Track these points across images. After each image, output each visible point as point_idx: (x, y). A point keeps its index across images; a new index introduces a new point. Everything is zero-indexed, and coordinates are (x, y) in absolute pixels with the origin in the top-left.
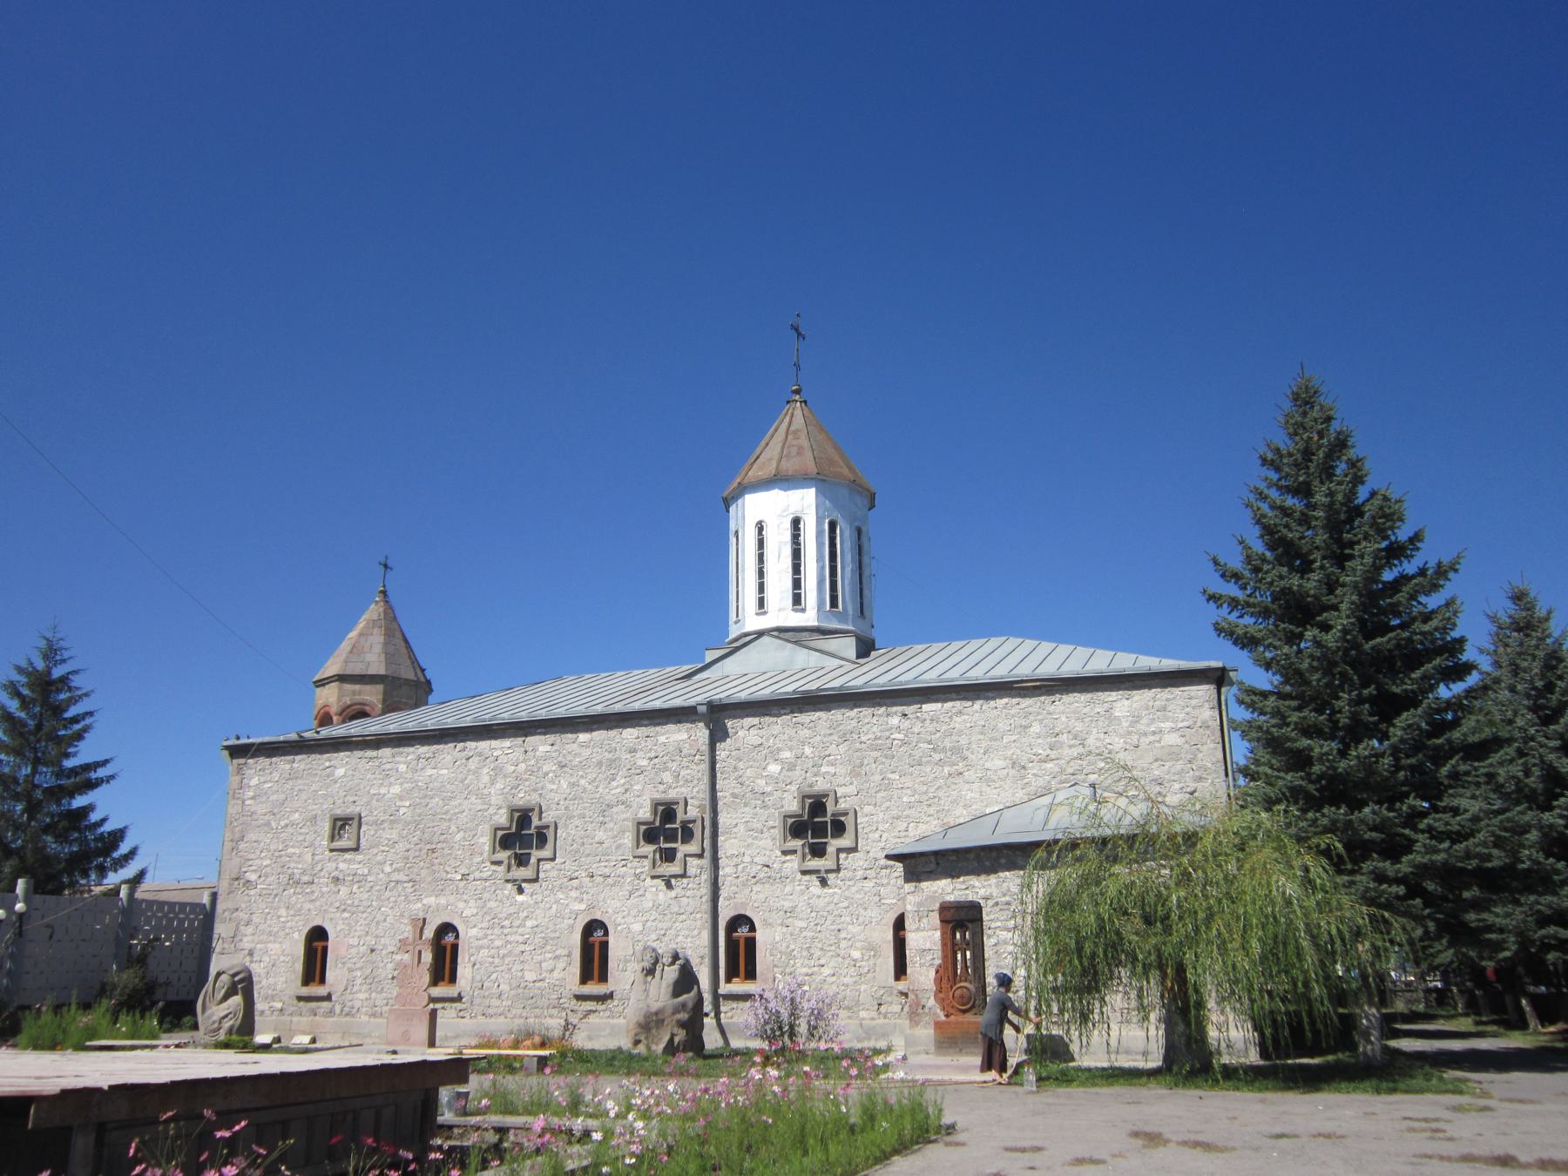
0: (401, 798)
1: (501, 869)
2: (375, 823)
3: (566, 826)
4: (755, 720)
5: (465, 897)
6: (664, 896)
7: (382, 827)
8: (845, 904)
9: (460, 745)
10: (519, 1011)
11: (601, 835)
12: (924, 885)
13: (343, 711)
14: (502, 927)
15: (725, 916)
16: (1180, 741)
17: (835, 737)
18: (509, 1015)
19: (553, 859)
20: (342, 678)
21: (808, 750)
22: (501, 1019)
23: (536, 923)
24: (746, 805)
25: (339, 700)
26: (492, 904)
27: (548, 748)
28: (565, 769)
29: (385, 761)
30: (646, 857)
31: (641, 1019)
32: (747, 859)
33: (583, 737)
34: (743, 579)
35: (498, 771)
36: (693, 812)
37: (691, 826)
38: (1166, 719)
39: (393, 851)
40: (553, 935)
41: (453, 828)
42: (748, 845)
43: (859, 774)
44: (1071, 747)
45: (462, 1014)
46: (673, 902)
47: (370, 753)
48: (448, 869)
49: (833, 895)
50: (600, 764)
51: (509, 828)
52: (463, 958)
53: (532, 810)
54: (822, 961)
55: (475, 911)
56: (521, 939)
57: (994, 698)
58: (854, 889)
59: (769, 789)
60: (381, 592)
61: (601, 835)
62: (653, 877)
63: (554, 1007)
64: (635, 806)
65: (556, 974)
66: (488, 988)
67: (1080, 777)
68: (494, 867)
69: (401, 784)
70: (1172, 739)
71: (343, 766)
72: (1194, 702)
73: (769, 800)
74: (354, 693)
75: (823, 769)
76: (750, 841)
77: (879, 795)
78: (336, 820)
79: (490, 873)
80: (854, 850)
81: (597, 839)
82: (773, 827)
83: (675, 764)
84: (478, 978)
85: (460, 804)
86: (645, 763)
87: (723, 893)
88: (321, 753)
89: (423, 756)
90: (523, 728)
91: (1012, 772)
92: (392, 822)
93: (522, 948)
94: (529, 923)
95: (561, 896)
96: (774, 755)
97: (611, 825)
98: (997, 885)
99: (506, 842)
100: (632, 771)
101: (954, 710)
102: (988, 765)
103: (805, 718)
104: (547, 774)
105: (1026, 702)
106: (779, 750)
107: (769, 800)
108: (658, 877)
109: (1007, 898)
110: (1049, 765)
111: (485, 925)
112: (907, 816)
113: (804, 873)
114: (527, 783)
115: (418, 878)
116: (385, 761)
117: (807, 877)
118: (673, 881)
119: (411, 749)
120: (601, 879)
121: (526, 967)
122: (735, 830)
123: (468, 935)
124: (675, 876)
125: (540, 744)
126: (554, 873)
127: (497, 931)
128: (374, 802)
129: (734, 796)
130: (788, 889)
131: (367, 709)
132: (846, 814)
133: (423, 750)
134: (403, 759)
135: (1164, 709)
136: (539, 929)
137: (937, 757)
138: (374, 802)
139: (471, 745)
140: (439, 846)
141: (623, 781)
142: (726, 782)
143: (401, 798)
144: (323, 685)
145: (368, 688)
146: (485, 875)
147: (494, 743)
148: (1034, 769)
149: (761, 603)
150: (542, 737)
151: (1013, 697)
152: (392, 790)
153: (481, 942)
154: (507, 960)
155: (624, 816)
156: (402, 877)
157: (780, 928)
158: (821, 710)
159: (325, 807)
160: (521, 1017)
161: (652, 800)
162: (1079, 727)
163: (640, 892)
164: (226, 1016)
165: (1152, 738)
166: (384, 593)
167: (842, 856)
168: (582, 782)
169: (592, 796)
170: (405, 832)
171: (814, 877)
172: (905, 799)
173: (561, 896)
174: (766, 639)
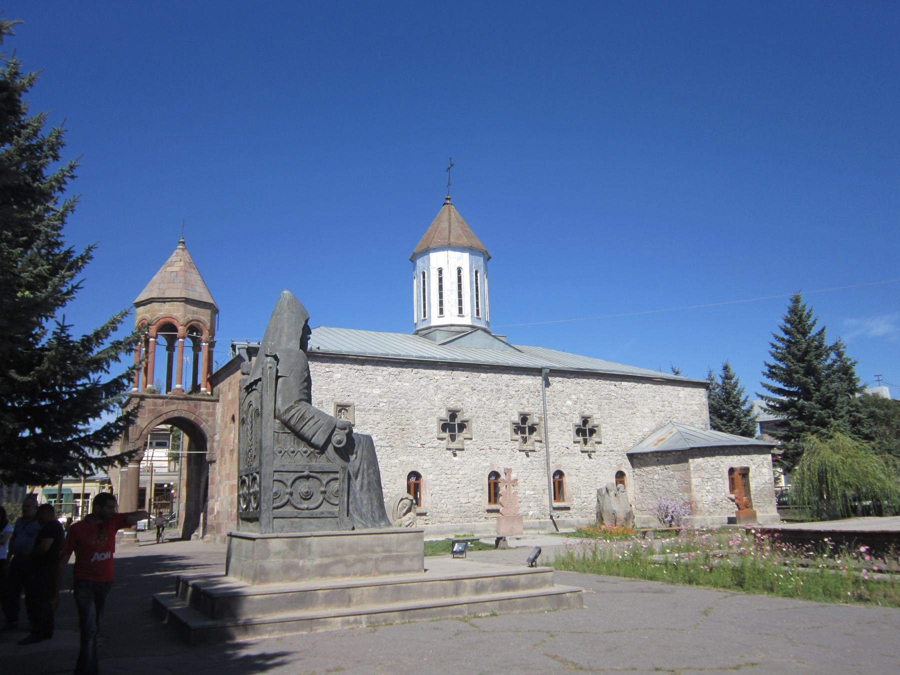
0: (380, 397)
1: (444, 442)
2: (364, 410)
3: (476, 422)
4: (561, 379)
5: (424, 457)
6: (526, 460)
7: (369, 413)
8: (598, 466)
9: (416, 370)
10: (459, 519)
11: (493, 427)
12: (695, 460)
13: (187, 324)
14: (446, 474)
15: (553, 470)
16: (697, 409)
17: (591, 392)
18: (453, 521)
19: (471, 439)
20: (187, 301)
21: (582, 396)
22: (450, 524)
23: (465, 472)
24: (558, 419)
25: (185, 316)
26: (440, 461)
27: (465, 379)
28: (474, 391)
29: (368, 373)
30: (517, 441)
31: (625, 516)
32: (560, 444)
33: (483, 375)
34: (429, 294)
35: (438, 387)
36: (536, 420)
37: (535, 427)
38: (694, 400)
39: (377, 428)
40: (473, 479)
41: (414, 417)
42: (561, 438)
43: (601, 410)
44: (668, 407)
45: (426, 522)
46: (530, 463)
47: (357, 367)
48: (413, 440)
49: (594, 462)
50: (492, 390)
51: (447, 420)
52: (426, 491)
53: (459, 411)
54: (591, 492)
55: (431, 465)
56: (457, 481)
57: (644, 384)
58: (601, 460)
59: (567, 412)
60: (183, 243)
61: (493, 427)
62: (520, 451)
63: (477, 516)
64: (510, 414)
65: (476, 499)
66: (441, 508)
67: (671, 419)
68: (440, 441)
69: (380, 388)
70: (695, 408)
71: (338, 373)
72: (701, 395)
73: (568, 417)
74: (194, 311)
75: (588, 405)
76: (561, 436)
77: (609, 419)
78: (338, 406)
79: (438, 444)
80: (599, 443)
81: (492, 430)
82: (570, 430)
83: (527, 395)
84: (435, 502)
85: (417, 404)
86: (514, 393)
87: (551, 460)
88: (322, 362)
89: (392, 373)
90: (452, 366)
91: (651, 415)
92: (375, 411)
93: (458, 485)
94: (461, 472)
95: (477, 458)
96: (569, 396)
97: (499, 423)
98: (716, 461)
99: (446, 426)
100: (508, 396)
101: (632, 386)
102: (644, 411)
103: (581, 381)
104: (465, 393)
105: (655, 387)
106: (571, 394)
107: (568, 417)
108: (523, 451)
109: (718, 466)
110: (662, 413)
111: (437, 473)
112: (618, 430)
113: (582, 452)
114: (455, 397)
115: (394, 445)
116: (368, 373)
117: (583, 454)
118: (529, 453)
119: (385, 368)
120: (496, 450)
121: (461, 495)
122: (554, 430)
123: (427, 479)
124: (531, 451)
125: (461, 376)
126: (472, 446)
127: (444, 476)
128: (363, 397)
129: (553, 414)
130: (576, 459)
131: (175, 323)
132: (597, 427)
133: (391, 369)
134: (381, 374)
135: (692, 396)
136: (466, 476)
137: (628, 405)
138: (363, 397)
139: (423, 371)
140: (406, 427)
141: (503, 401)
142: (550, 407)
143: (380, 397)
144: (164, 302)
145: (202, 310)
146: (435, 445)
147: (435, 372)
148: (657, 414)
149: (460, 311)
150: (461, 372)
151: (651, 384)
152: (374, 391)
153: (435, 482)
154: (450, 492)
155: (504, 419)
156: (383, 443)
157: (574, 477)
158: (585, 378)
159: (328, 397)
160: (460, 522)
161: (519, 412)
162: (670, 399)
163: (515, 458)
164: (409, 525)
165: (690, 407)
166: (183, 243)
167: (597, 445)
168: (484, 399)
169: (489, 407)
170: (384, 417)
171: (586, 454)
172: (617, 422)
173: (477, 458)
174: (480, 332)
